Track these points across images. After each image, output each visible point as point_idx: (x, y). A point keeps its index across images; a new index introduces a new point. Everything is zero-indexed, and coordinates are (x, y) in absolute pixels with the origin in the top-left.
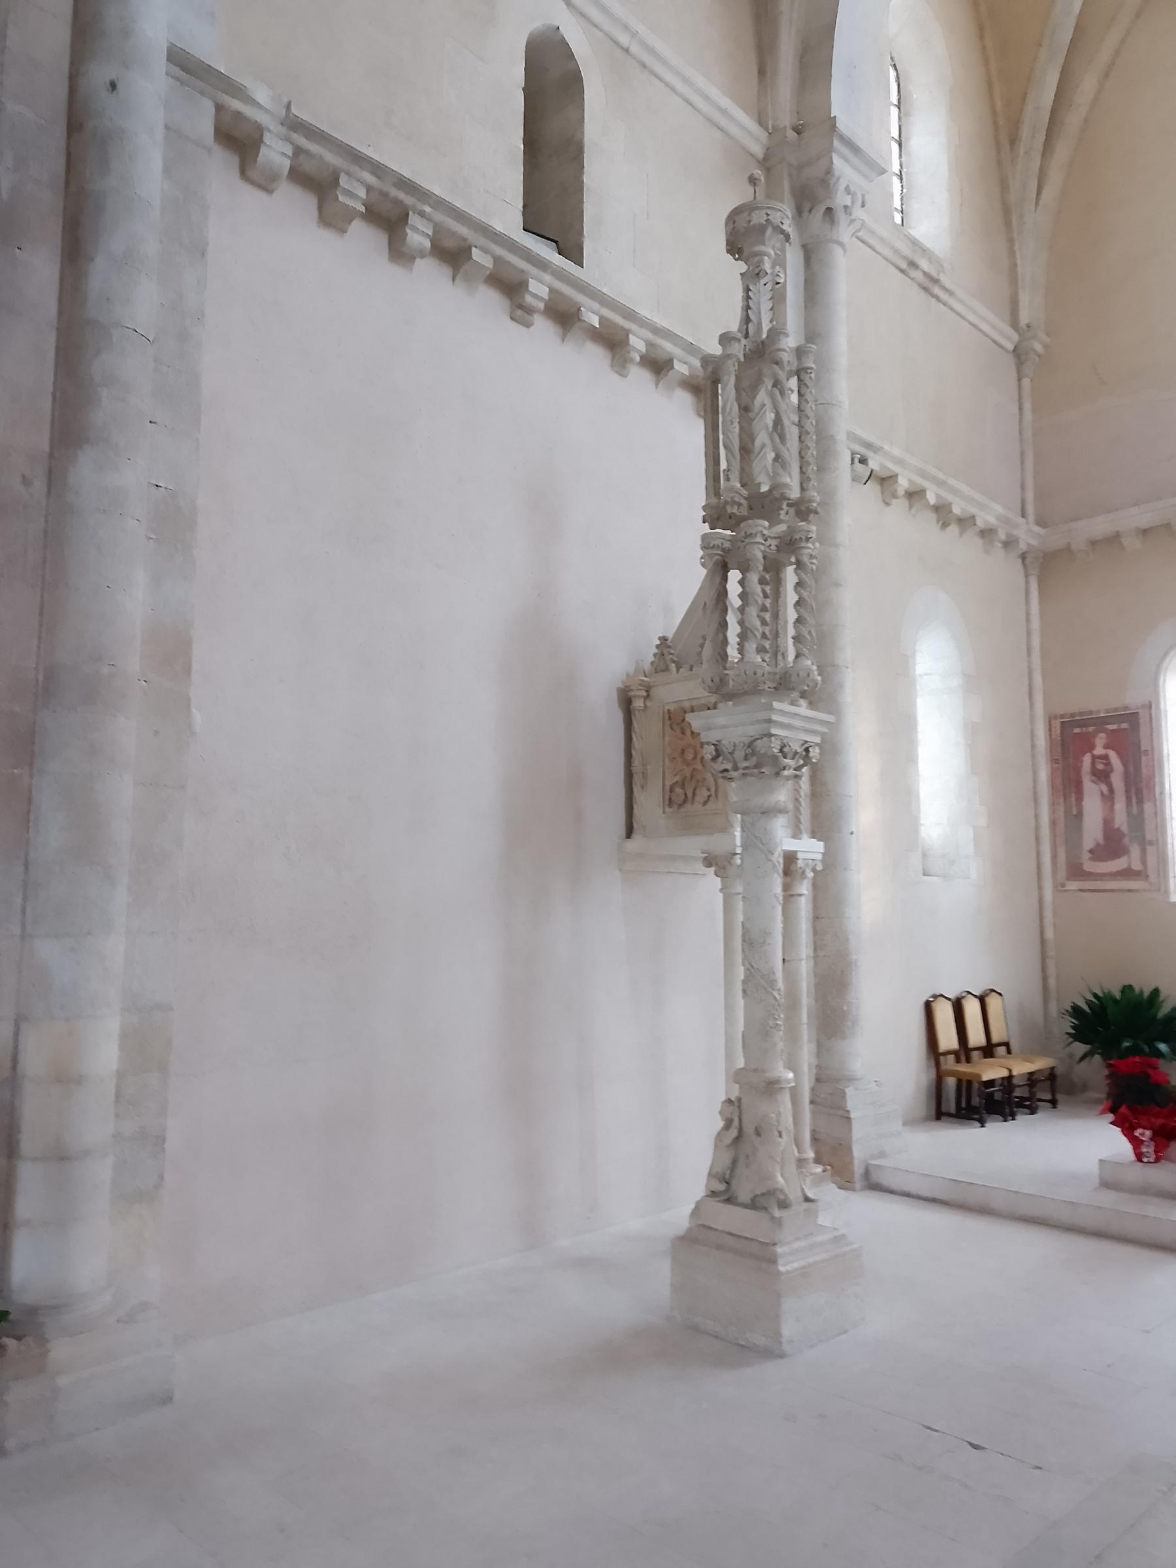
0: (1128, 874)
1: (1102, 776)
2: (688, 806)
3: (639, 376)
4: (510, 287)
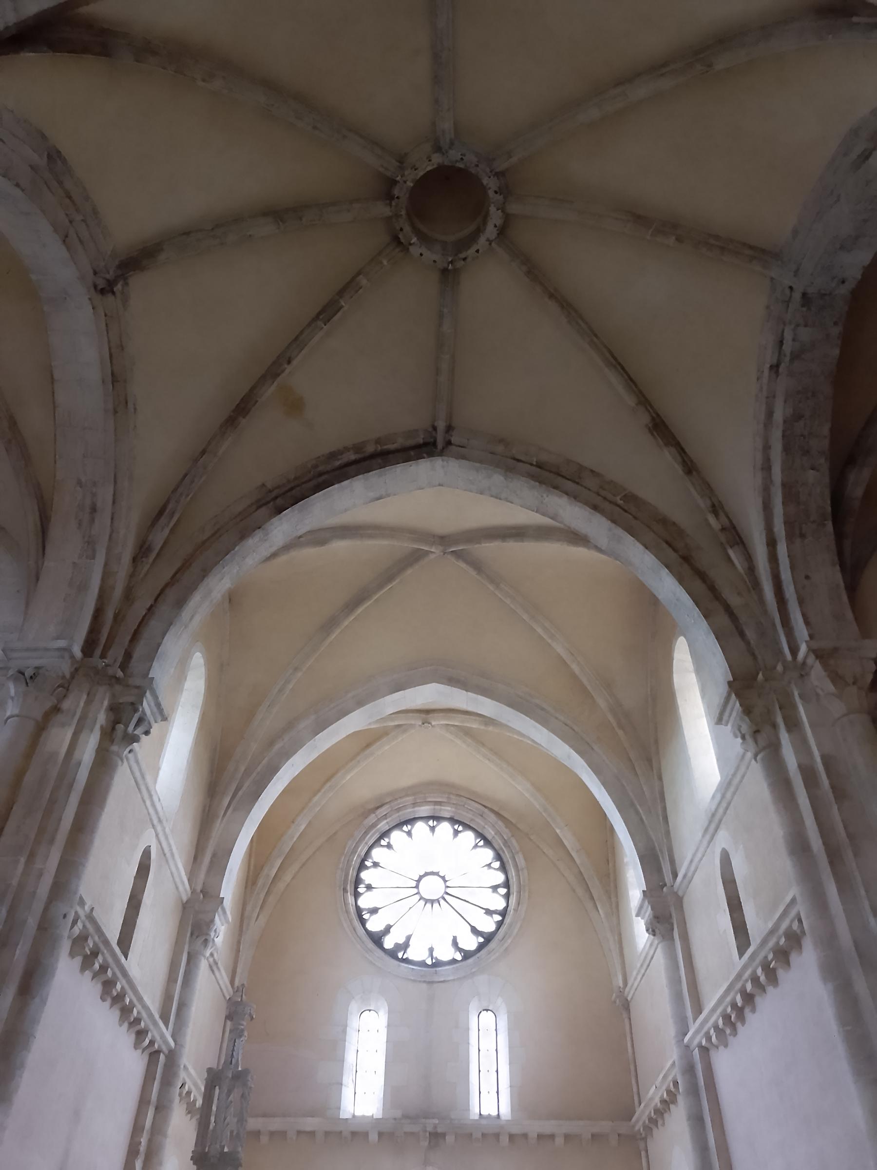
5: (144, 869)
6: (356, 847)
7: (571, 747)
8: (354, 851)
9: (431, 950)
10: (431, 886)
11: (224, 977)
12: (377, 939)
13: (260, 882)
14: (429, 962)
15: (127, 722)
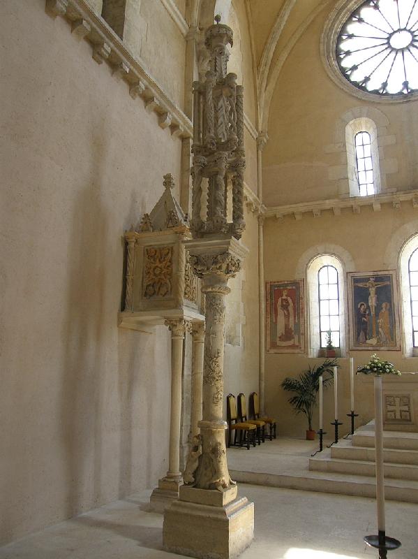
0: (293, 346)
1: (285, 307)
2: (155, 296)
3: (139, 101)
4: (95, 44)
6: (333, 25)
8: (331, 29)
12: (360, 87)
13: (263, 62)
14: (405, 92)
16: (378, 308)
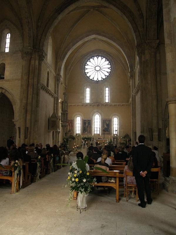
5: (48, 74)
7: (120, 46)
9: (98, 79)
10: (98, 68)
11: (63, 85)
14: (97, 80)
15: (42, 57)
16: (88, 126)
